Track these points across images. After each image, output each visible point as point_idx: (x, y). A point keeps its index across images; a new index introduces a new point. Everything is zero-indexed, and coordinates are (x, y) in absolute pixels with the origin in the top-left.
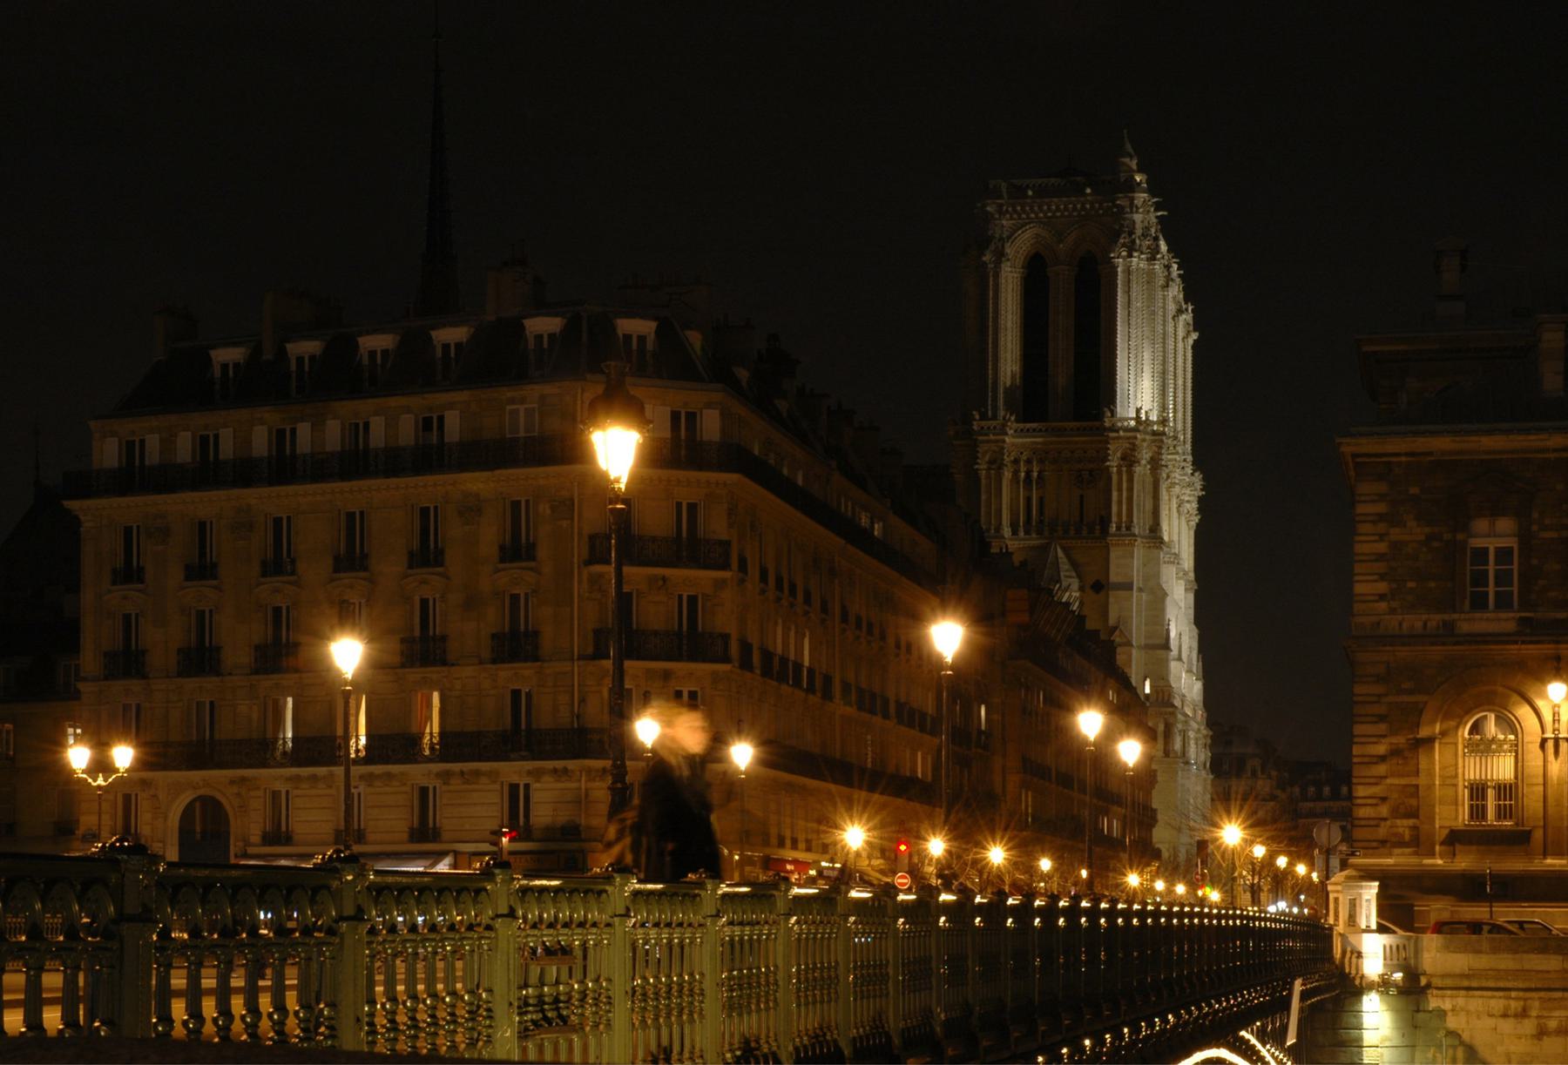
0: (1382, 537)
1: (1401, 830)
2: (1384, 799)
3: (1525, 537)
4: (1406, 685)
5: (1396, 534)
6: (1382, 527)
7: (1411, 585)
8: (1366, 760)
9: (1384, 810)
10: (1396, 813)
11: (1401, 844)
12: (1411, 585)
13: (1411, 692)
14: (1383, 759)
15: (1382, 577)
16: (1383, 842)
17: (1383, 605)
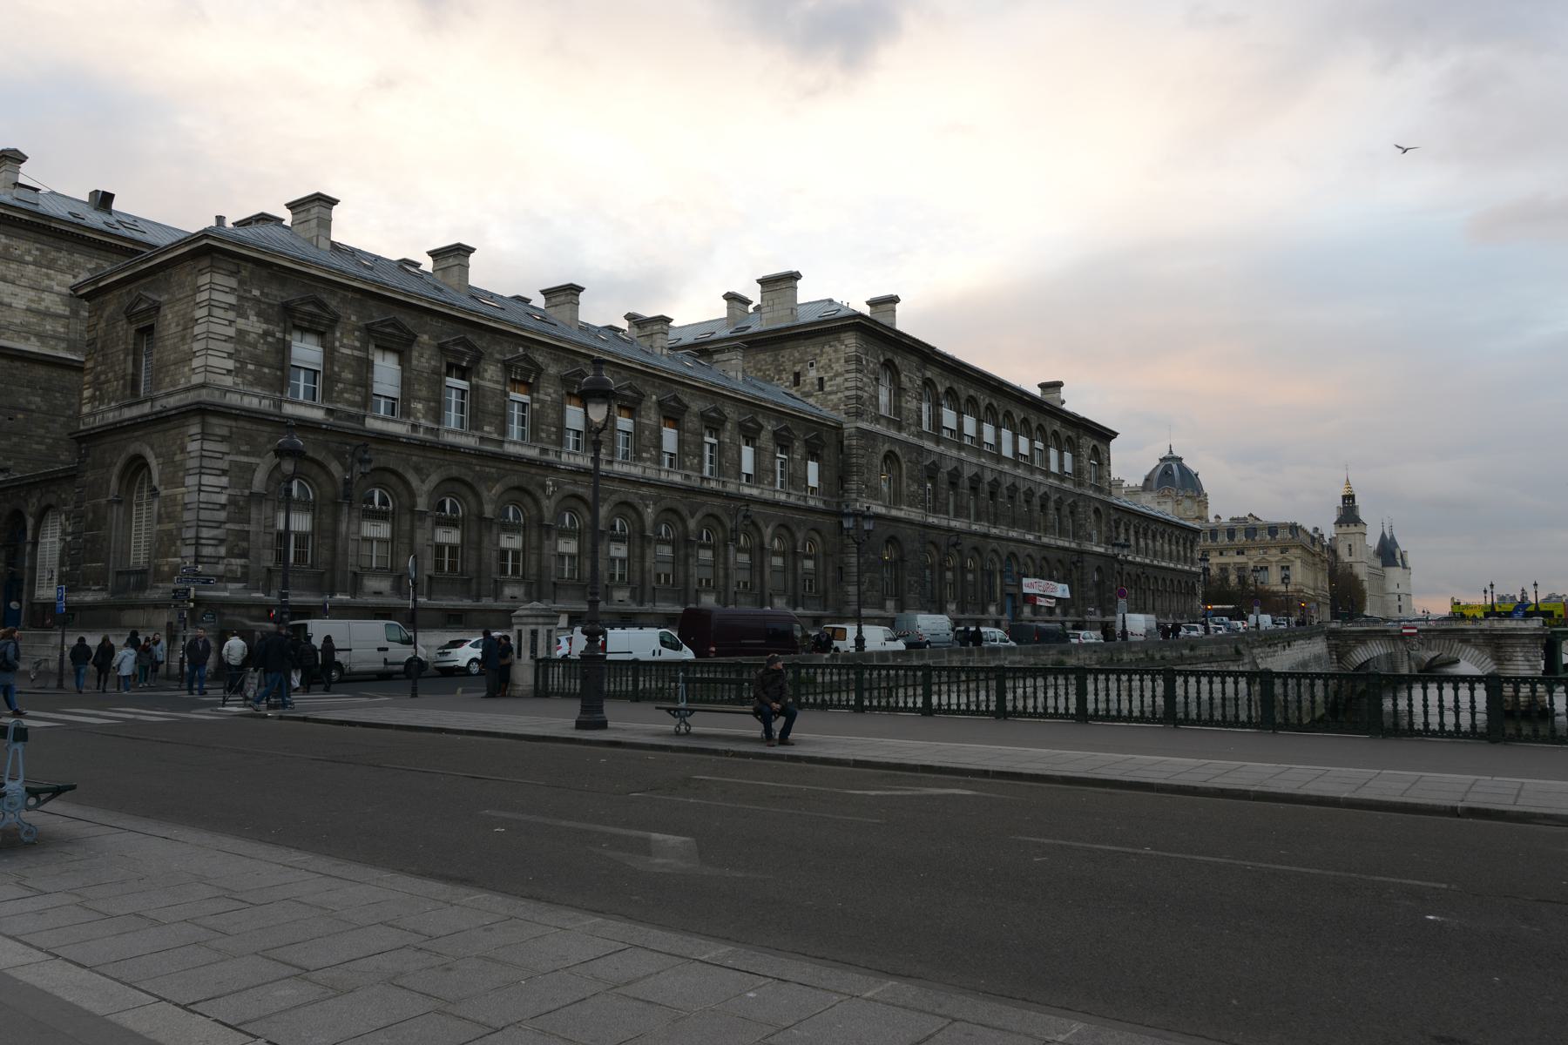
0: (231, 322)
1: (234, 568)
2: (221, 541)
3: (330, 354)
4: (244, 448)
5: (241, 323)
6: (231, 315)
7: (251, 367)
8: (210, 506)
9: (222, 551)
10: (230, 554)
11: (235, 580)
12: (251, 367)
13: (247, 454)
14: (223, 507)
15: (230, 356)
16: (220, 578)
17: (228, 381)
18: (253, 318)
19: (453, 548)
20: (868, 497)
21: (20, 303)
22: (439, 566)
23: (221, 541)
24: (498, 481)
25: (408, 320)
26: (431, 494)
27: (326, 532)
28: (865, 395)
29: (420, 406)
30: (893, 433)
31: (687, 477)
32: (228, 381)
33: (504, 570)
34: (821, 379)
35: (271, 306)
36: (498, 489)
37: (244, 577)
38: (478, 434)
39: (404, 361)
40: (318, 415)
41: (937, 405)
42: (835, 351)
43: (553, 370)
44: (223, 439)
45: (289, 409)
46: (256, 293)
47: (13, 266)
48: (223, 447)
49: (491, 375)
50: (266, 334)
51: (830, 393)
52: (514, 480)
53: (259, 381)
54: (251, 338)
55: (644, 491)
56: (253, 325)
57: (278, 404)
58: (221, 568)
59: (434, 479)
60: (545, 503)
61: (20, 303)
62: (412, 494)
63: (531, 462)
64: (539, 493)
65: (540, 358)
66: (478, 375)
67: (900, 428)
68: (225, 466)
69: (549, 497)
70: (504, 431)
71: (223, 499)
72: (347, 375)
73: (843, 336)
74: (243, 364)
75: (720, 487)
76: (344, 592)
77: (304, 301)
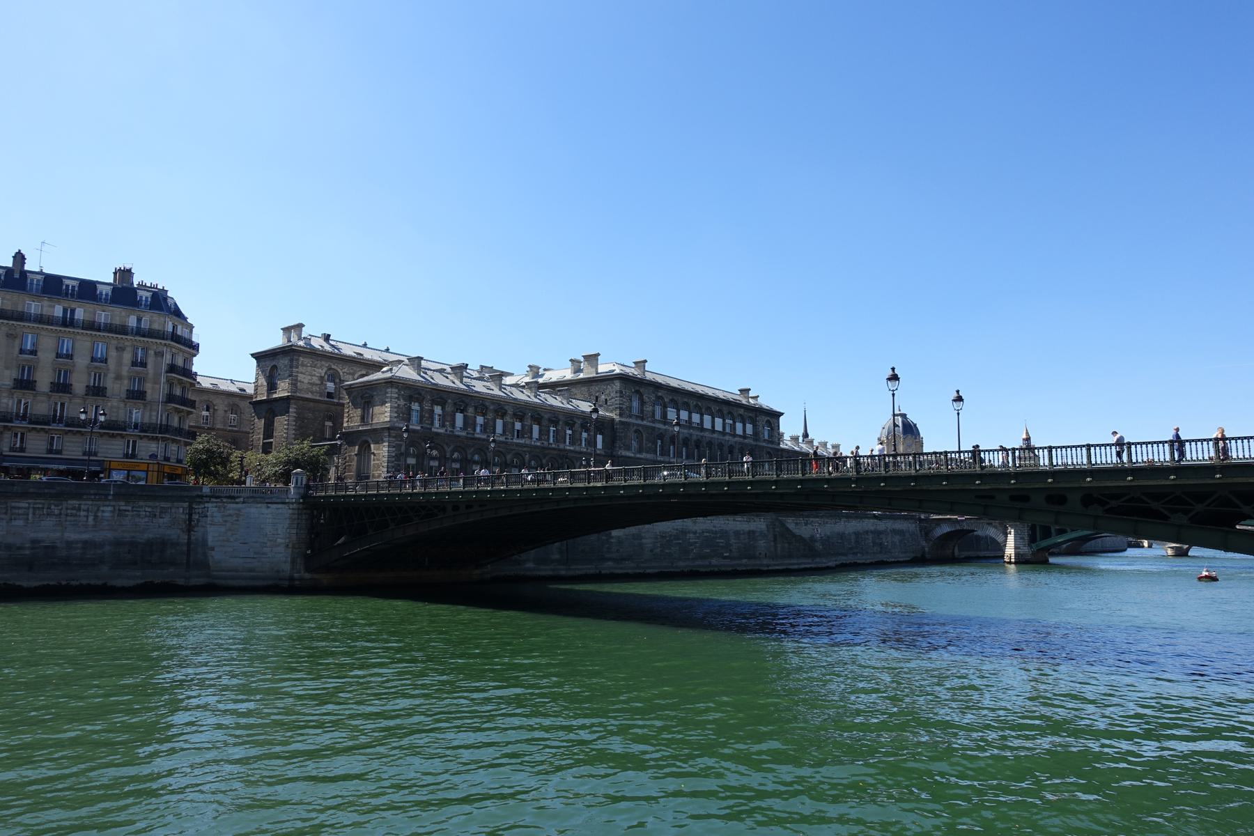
6: (396, 400)
14: (394, 457)
15: (396, 412)
17: (395, 420)
20: (625, 450)
21: (306, 381)
23: (393, 467)
28: (624, 407)
29: (448, 423)
30: (639, 422)
31: (542, 443)
34: (606, 400)
41: (665, 407)
42: (612, 388)
46: (403, 393)
47: (305, 368)
49: (471, 411)
50: (405, 404)
51: (610, 405)
53: (403, 419)
55: (525, 449)
56: (402, 402)
61: (306, 381)
62: (445, 452)
67: (643, 419)
68: (394, 445)
70: (475, 430)
72: (427, 415)
73: (615, 382)
75: (557, 447)
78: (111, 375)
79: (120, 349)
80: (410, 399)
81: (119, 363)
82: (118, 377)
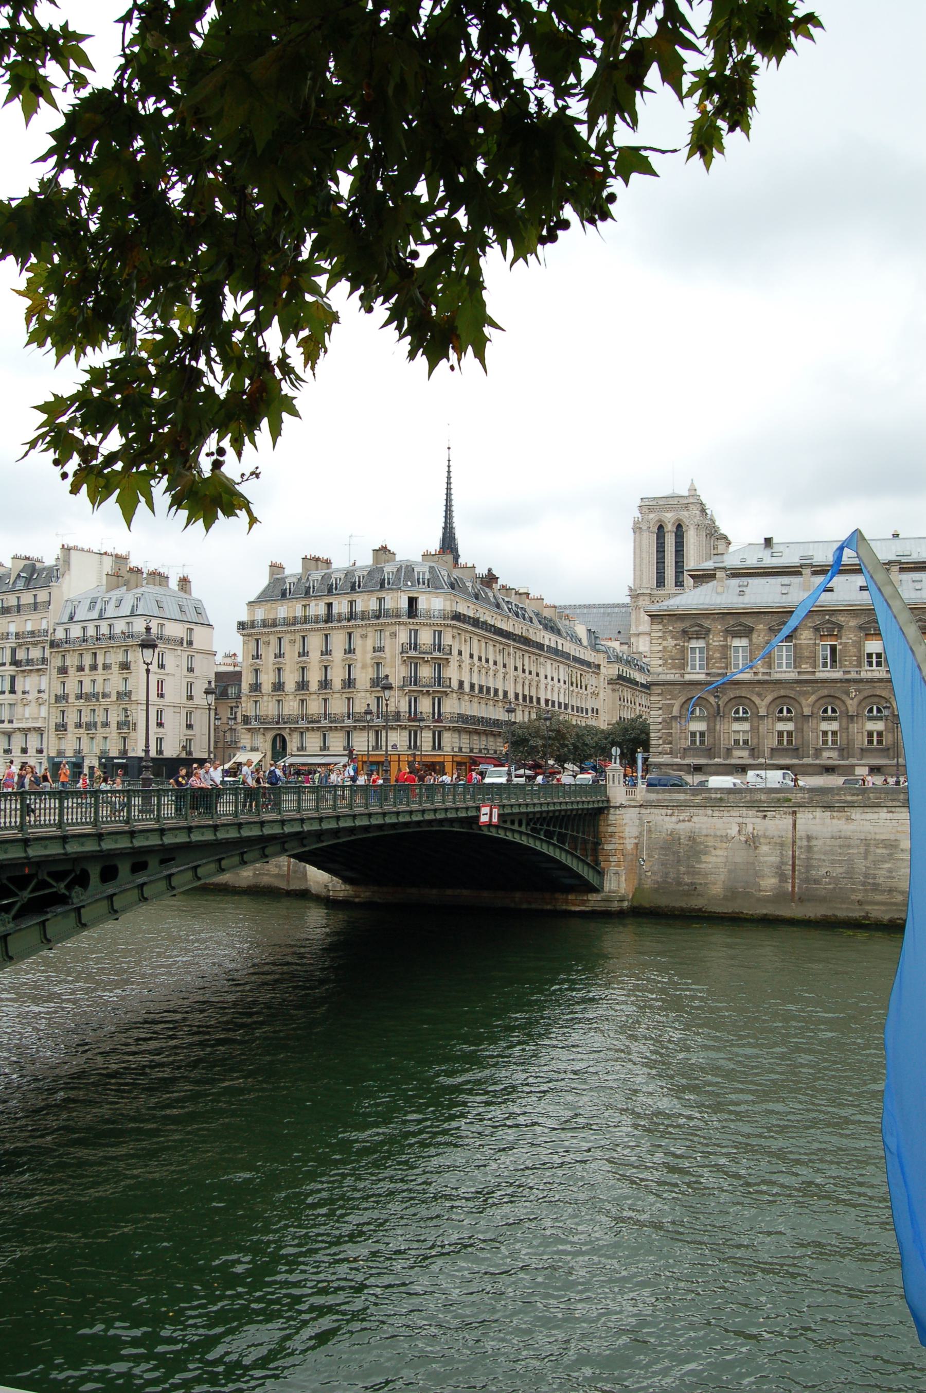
2: (660, 738)
5: (665, 643)
6: (660, 641)
9: (661, 742)
10: (664, 743)
14: (660, 723)
16: (660, 753)
17: (660, 669)
18: (670, 640)
19: (790, 734)
22: (780, 742)
23: (660, 738)
24: (813, 694)
25: (749, 621)
26: (768, 706)
27: (712, 729)
32: (660, 669)
33: (825, 742)
35: (677, 632)
36: (813, 698)
37: (671, 753)
38: (799, 670)
39: (751, 640)
40: (702, 677)
43: (853, 623)
44: (659, 694)
45: (688, 677)
46: (671, 628)
48: (659, 698)
50: (676, 645)
52: (825, 692)
54: (669, 649)
56: (670, 642)
57: (682, 675)
58: (660, 749)
59: (769, 698)
60: (849, 702)
63: (834, 681)
64: (844, 697)
65: (841, 619)
66: (796, 639)
69: (852, 699)
71: (660, 720)
74: (666, 660)
76: (720, 757)
77: (691, 626)
78: (359, 665)
79: (364, 637)
80: (686, 634)
81: (364, 652)
82: (364, 667)
